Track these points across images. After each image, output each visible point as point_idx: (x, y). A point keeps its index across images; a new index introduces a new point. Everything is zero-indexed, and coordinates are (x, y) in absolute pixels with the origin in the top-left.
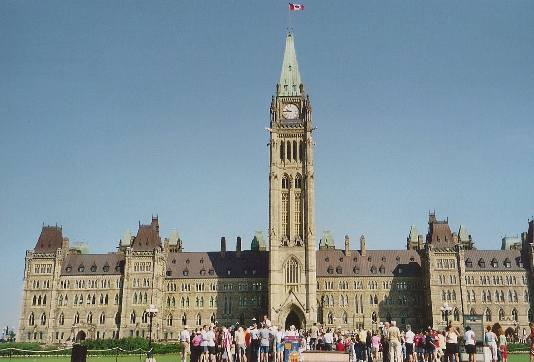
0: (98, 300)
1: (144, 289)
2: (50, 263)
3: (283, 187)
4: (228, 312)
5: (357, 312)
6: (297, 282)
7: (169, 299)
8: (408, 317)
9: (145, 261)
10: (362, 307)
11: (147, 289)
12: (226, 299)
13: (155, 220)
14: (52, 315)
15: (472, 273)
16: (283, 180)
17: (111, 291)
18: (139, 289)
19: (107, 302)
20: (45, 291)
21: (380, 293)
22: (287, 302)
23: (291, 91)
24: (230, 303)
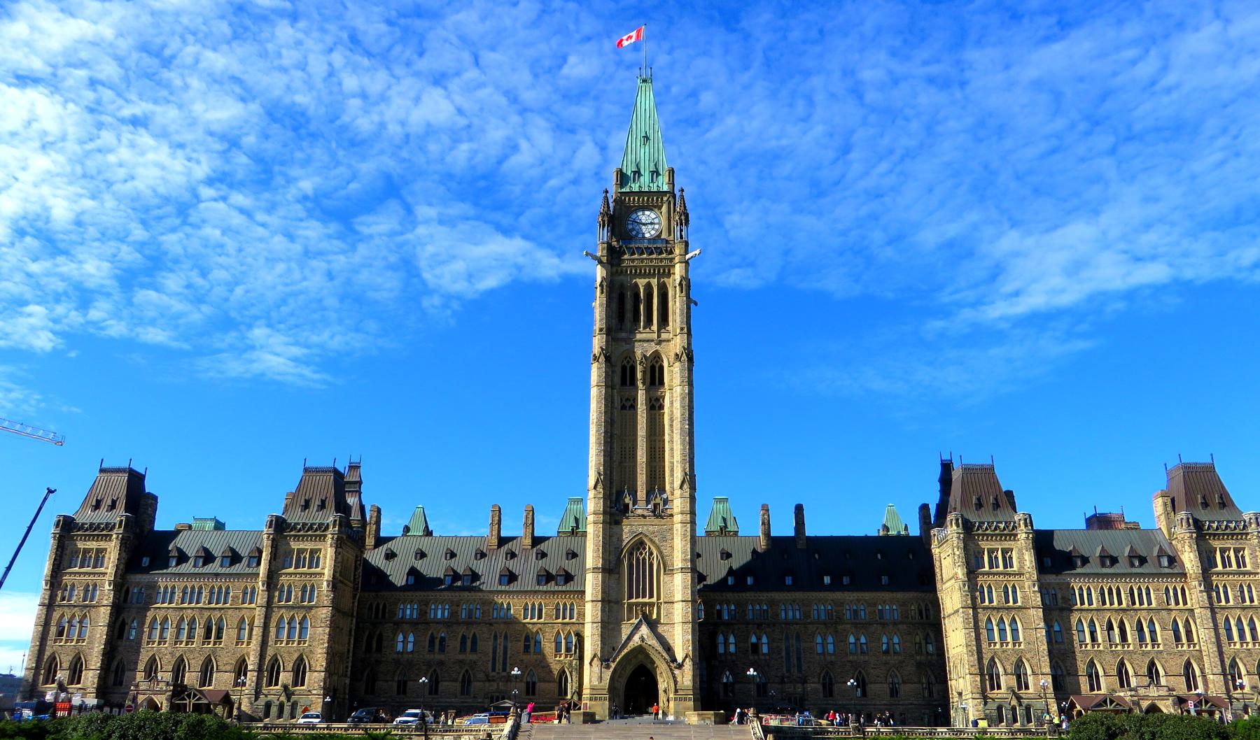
0: (199, 631)
1: (303, 607)
2: (103, 545)
3: (623, 383)
4: (499, 666)
5: (789, 671)
6: (651, 596)
7: (370, 638)
8: (904, 682)
9: (309, 546)
10: (799, 659)
11: (311, 608)
12: (495, 637)
13: (354, 467)
14: (95, 661)
15: (1051, 579)
16: (624, 368)
17: (230, 612)
18: (292, 607)
19: (219, 636)
20: (86, 606)
21: (840, 627)
22: (631, 645)
23: (644, 183)
24: (505, 648)
